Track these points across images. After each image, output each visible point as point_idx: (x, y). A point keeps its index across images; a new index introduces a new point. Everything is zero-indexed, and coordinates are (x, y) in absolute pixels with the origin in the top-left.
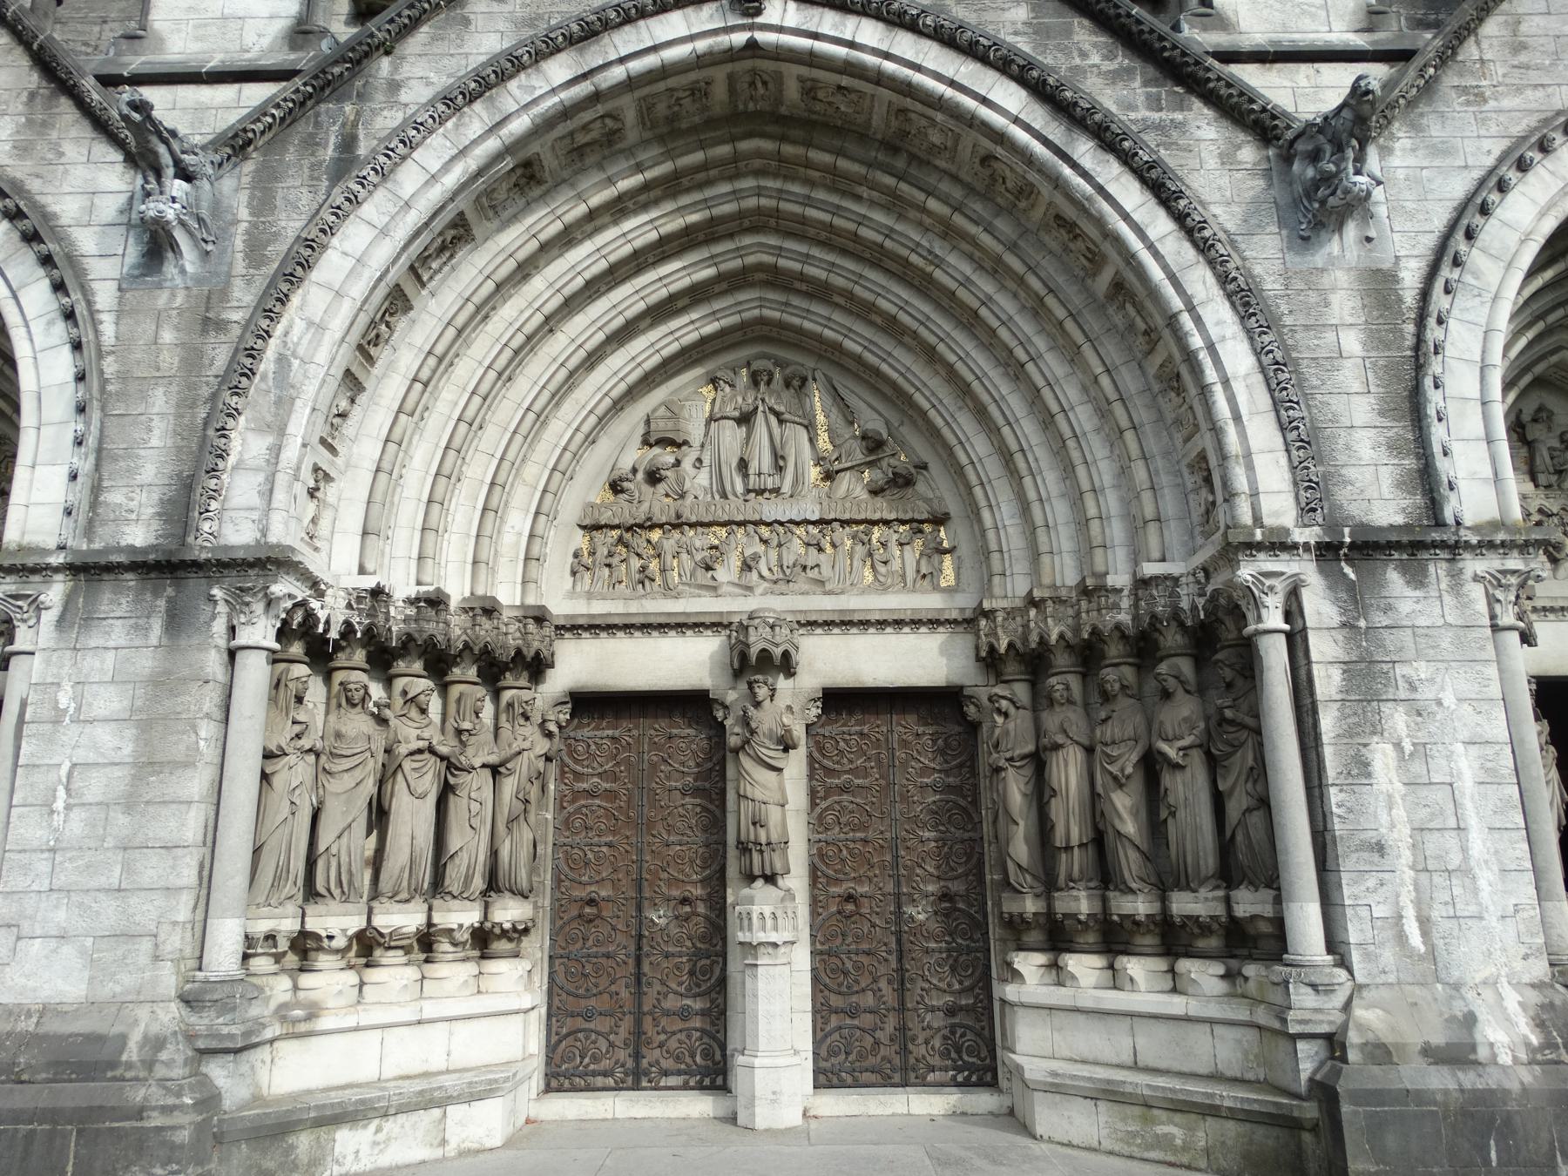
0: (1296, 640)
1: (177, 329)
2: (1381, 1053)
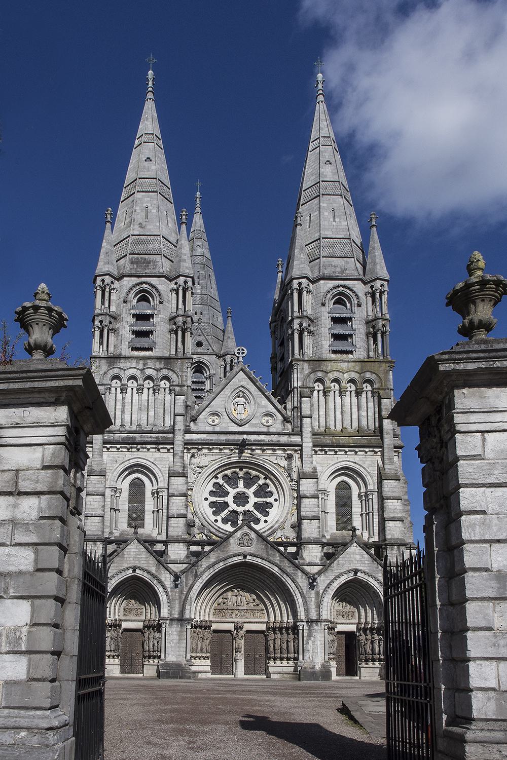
0: (303, 630)
2: (305, 668)
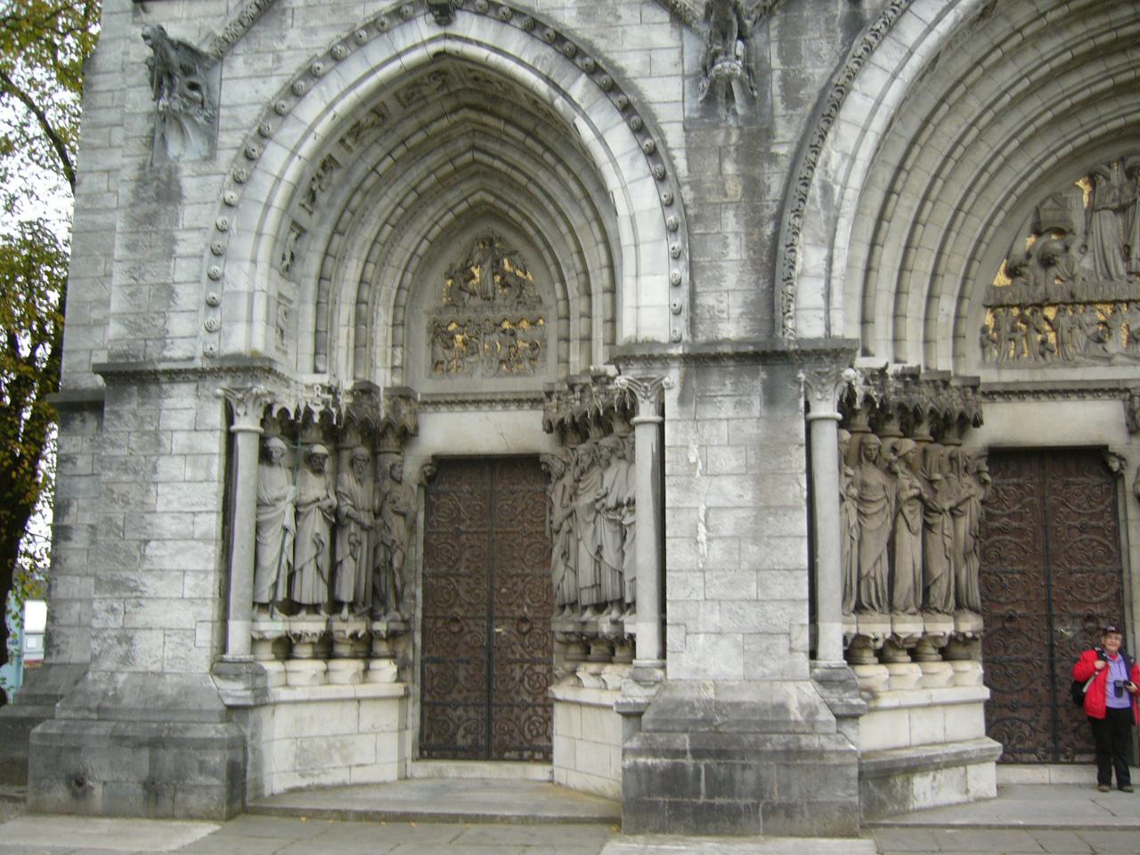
1: (736, 162)
